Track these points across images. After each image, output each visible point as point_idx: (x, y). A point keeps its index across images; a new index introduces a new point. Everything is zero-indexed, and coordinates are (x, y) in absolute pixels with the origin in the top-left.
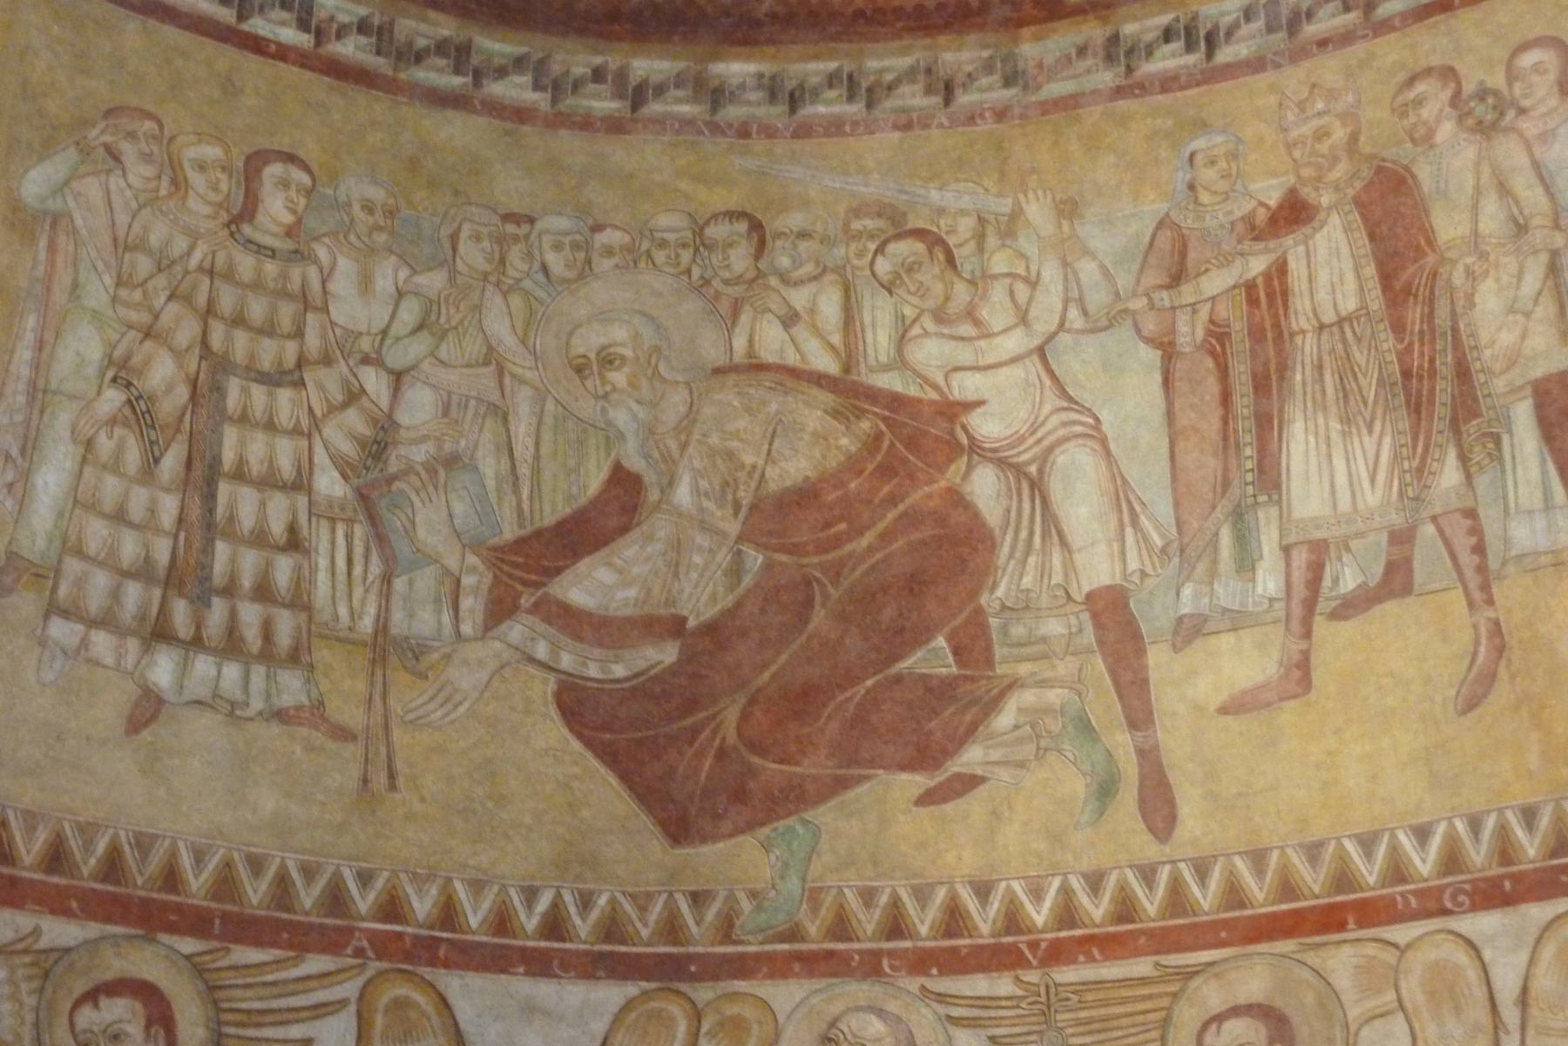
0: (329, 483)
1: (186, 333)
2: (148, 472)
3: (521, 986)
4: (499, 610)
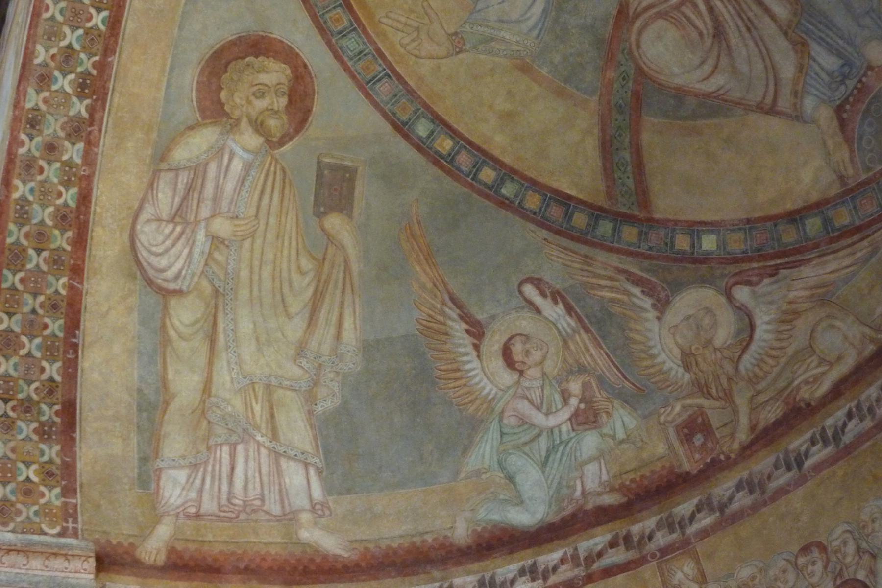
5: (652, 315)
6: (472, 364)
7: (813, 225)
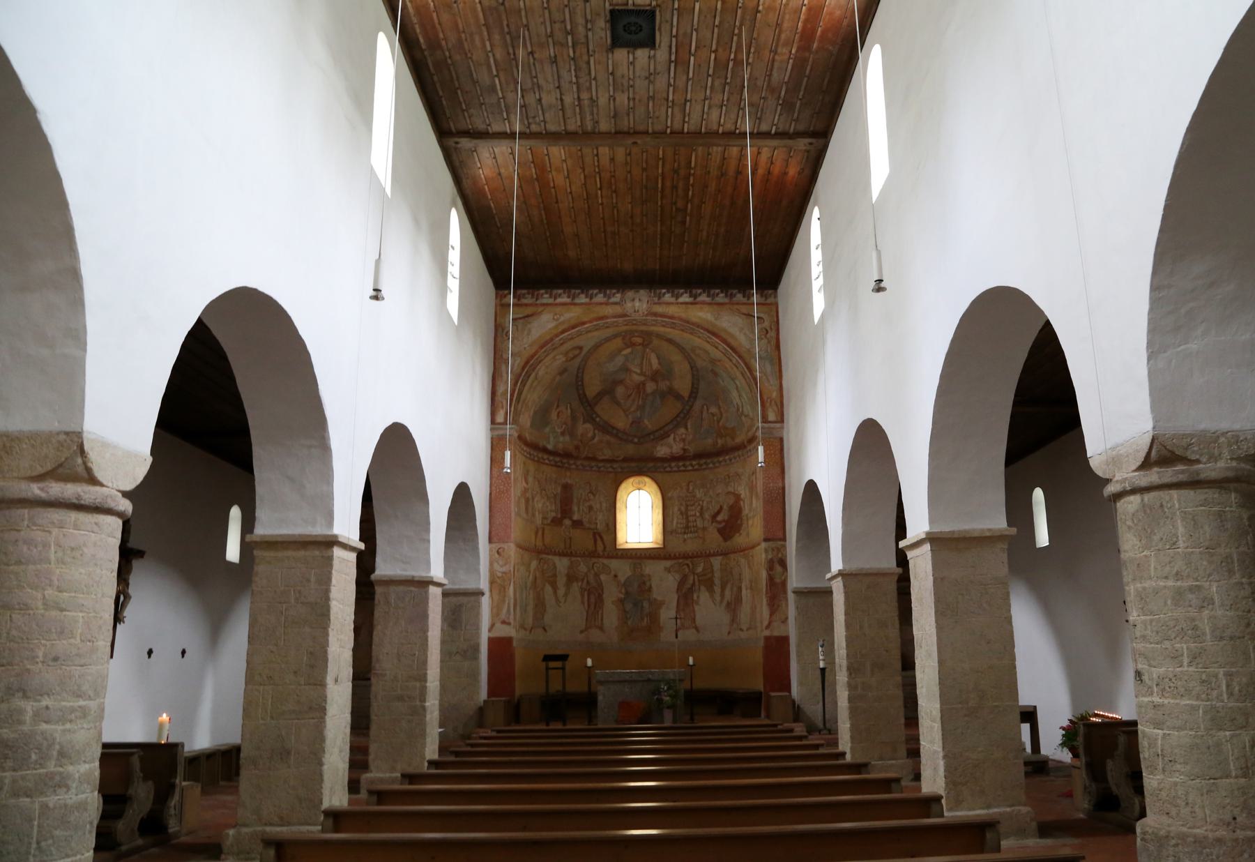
0: (698, 514)
1: (684, 504)
2: (683, 518)
4: (712, 522)
5: (581, 423)
6: (554, 410)
7: (615, 431)
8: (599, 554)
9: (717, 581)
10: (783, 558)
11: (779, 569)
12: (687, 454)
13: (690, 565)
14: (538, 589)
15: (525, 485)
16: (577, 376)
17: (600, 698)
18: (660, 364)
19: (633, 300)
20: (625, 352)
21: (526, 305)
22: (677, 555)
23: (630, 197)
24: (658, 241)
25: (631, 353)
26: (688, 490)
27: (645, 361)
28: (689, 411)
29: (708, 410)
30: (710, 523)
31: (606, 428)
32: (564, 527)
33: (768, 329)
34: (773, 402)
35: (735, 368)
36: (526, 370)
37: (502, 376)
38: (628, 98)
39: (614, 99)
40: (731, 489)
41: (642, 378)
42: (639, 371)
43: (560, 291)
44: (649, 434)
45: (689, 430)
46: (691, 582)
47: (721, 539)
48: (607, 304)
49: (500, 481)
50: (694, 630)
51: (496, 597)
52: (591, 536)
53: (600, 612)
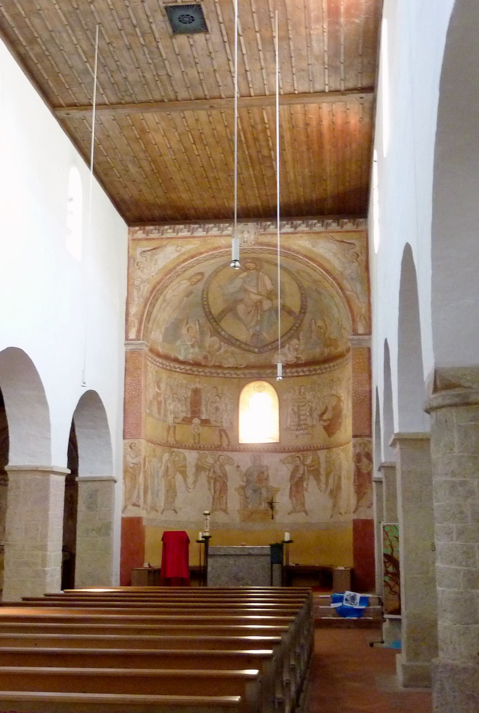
0: (308, 414)
3: (322, 451)
7: (238, 343)
8: (224, 448)
9: (323, 471)
10: (369, 452)
11: (365, 460)
12: (300, 362)
13: (302, 459)
14: (170, 478)
15: (158, 391)
16: (202, 298)
17: (209, 569)
18: (273, 285)
19: (243, 232)
20: (241, 276)
21: (153, 239)
22: (291, 448)
23: (220, 148)
24: (254, 183)
25: (247, 276)
26: (300, 392)
27: (260, 283)
28: (300, 324)
29: (315, 324)
30: (318, 421)
31: (231, 341)
32: (193, 425)
33: (359, 254)
34: (362, 317)
35: (332, 288)
36: (153, 295)
37: (134, 300)
38: (198, 73)
39: (187, 74)
40: (334, 392)
41: (259, 297)
42: (255, 291)
43: (182, 226)
44: (267, 345)
45: (302, 341)
46: (301, 472)
47: (326, 435)
48: (220, 236)
49: (133, 388)
50: (304, 514)
51: (128, 484)
52: (217, 433)
53: (224, 498)
